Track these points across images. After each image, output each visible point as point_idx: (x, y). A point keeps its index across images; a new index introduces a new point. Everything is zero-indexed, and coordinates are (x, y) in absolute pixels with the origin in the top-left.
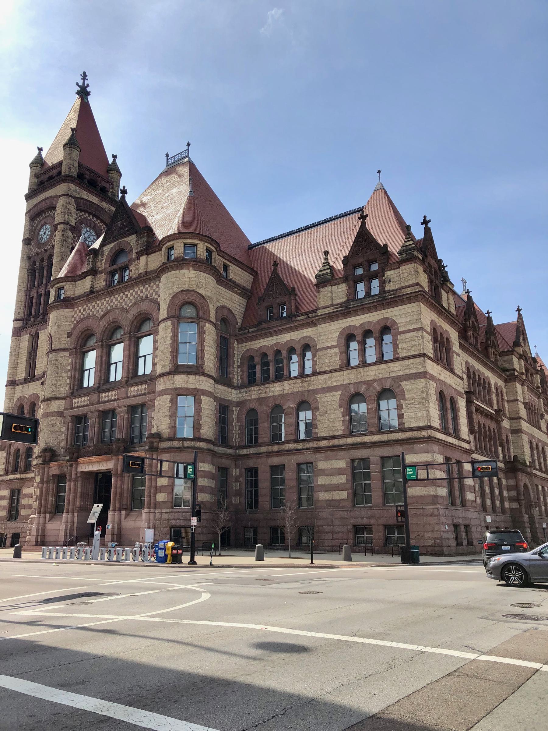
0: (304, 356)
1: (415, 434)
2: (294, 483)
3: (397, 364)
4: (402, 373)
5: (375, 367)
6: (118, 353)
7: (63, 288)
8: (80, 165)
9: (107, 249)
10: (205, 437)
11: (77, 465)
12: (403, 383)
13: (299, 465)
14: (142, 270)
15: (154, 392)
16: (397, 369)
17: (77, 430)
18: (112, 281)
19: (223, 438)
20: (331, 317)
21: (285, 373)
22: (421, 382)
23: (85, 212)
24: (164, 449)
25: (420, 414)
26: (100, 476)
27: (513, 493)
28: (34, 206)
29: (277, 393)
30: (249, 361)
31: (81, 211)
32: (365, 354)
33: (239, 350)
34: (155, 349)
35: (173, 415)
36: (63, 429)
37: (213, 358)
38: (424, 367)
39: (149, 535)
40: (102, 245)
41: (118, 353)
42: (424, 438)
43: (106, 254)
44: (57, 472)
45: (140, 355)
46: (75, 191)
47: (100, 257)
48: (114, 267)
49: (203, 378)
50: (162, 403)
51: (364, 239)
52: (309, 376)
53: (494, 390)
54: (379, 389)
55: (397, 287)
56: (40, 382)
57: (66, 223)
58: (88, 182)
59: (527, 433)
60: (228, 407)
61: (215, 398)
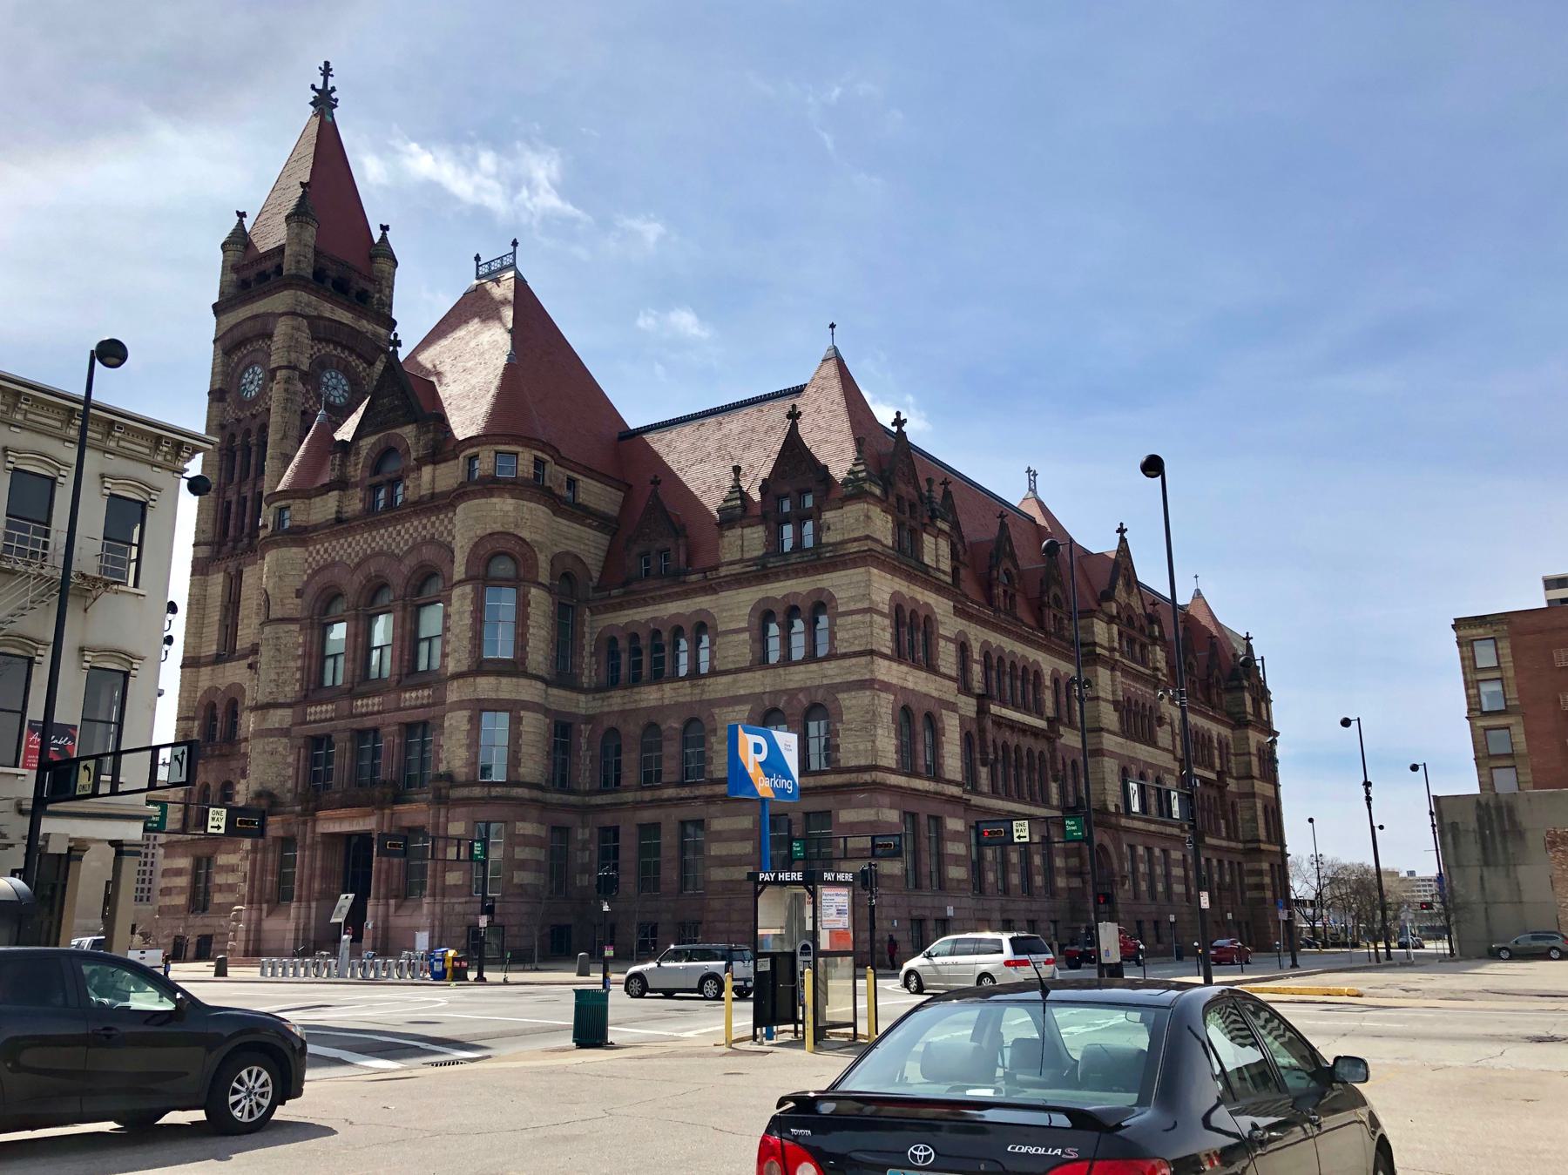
0: (699, 641)
1: (853, 777)
2: (674, 853)
3: (833, 664)
4: (838, 680)
5: (802, 668)
6: (382, 630)
7: (288, 507)
8: (318, 253)
9: (366, 443)
10: (528, 779)
11: (315, 821)
12: (840, 696)
13: (683, 823)
14: (425, 490)
15: (444, 703)
16: (833, 672)
17: (315, 760)
18: (375, 502)
19: (560, 776)
20: (739, 581)
21: (667, 669)
22: (865, 697)
23: (328, 341)
24: (459, 799)
25: (861, 747)
26: (355, 840)
27: (1074, 862)
28: (231, 329)
29: (652, 703)
30: (609, 647)
31: (320, 340)
32: (789, 643)
33: (594, 625)
34: (446, 629)
35: (474, 743)
36: (290, 759)
37: (542, 645)
38: (872, 671)
39: (422, 941)
40: (359, 433)
41: (382, 630)
42: (866, 784)
43: (364, 453)
44: (281, 833)
45: (422, 635)
46: (309, 305)
47: (352, 458)
48: (378, 479)
49: (523, 681)
50: (457, 722)
51: (794, 454)
52: (704, 676)
53: (1048, 683)
54: (806, 703)
55: (839, 538)
56: (244, 663)
57: (291, 367)
58: (334, 284)
59: (1113, 755)
60: (570, 725)
61: (547, 712)
